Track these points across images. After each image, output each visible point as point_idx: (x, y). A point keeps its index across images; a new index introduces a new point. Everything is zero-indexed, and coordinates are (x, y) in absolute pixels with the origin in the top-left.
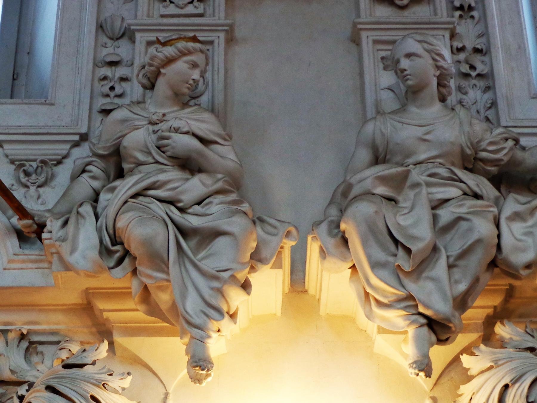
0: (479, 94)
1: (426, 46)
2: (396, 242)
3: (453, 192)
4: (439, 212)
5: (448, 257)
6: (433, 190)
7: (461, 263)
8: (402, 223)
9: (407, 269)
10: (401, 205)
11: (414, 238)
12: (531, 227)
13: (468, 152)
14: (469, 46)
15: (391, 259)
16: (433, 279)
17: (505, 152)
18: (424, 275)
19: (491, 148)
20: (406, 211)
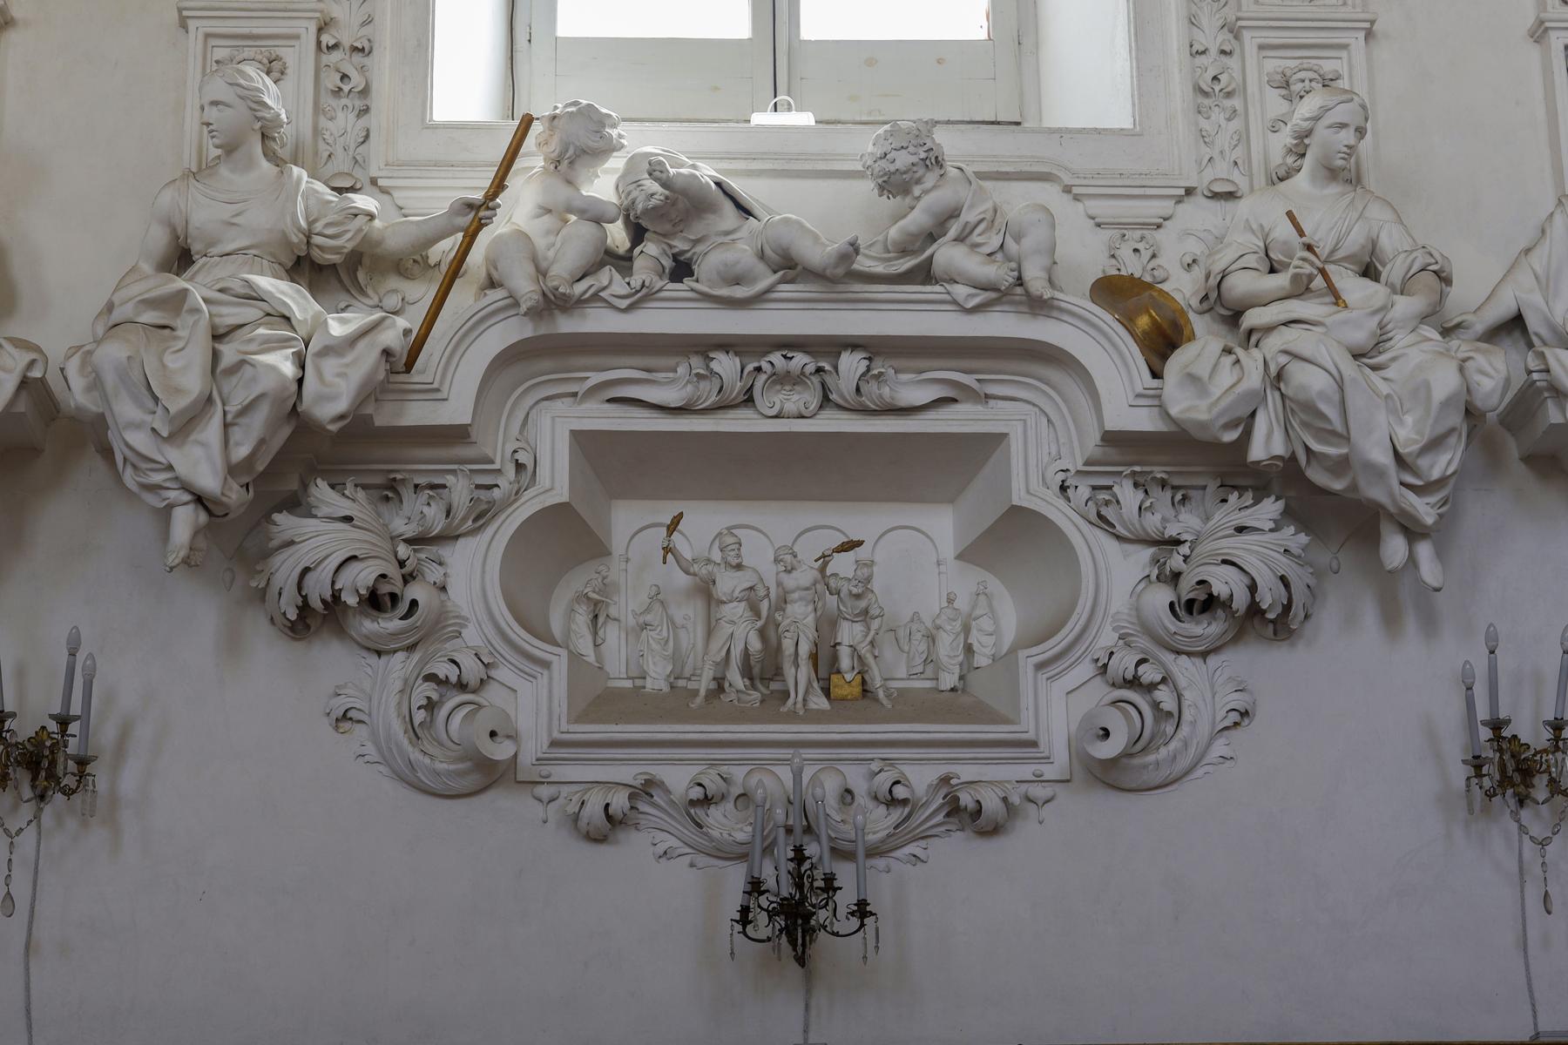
0: (352, 117)
1: (239, 90)
2: (156, 399)
3: (250, 313)
4: (222, 347)
5: (225, 413)
6: (224, 310)
7: (241, 420)
8: (170, 365)
9: (165, 434)
10: (179, 333)
11: (178, 391)
12: (347, 365)
13: (295, 240)
14: (346, 42)
15: (149, 418)
16: (202, 444)
17: (349, 235)
18: (192, 437)
19: (329, 231)
20: (181, 344)
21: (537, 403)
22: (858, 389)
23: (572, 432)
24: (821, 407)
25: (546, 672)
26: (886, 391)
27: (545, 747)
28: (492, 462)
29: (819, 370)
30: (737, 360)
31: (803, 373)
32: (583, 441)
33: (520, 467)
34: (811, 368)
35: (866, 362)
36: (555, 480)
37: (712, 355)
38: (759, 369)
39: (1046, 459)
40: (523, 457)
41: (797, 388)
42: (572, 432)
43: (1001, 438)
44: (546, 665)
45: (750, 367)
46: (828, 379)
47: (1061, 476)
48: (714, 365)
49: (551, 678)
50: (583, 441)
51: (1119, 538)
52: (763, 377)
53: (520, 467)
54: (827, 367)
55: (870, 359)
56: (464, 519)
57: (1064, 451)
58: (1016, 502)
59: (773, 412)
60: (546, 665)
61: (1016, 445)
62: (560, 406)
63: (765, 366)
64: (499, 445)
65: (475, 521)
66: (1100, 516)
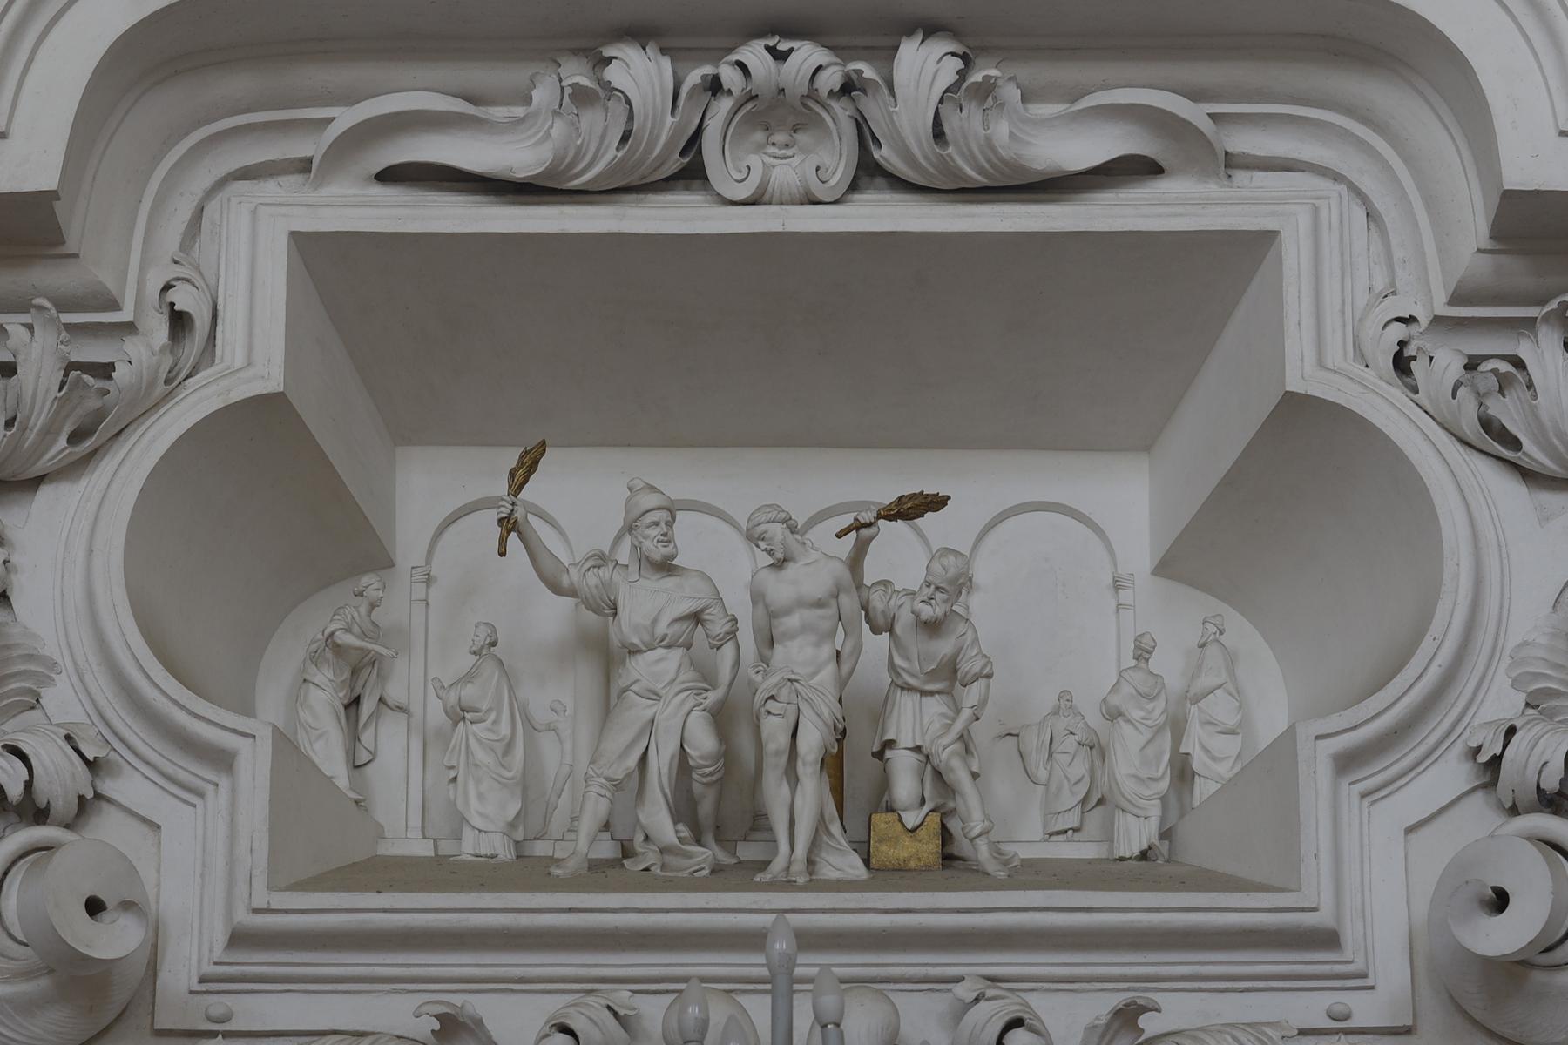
21: (221, 183)
22: (938, 134)
23: (295, 236)
24: (854, 187)
25: (224, 782)
26: (1001, 130)
27: (218, 953)
28: (115, 306)
29: (848, 88)
30: (666, 63)
31: (812, 94)
32: (315, 253)
33: (179, 321)
34: (831, 79)
35: (958, 64)
36: (255, 345)
37: (608, 52)
38: (714, 86)
39: (1362, 299)
40: (182, 298)
41: (802, 138)
42: (295, 236)
43: (1268, 238)
44: (222, 760)
45: (694, 77)
46: (873, 108)
47: (1399, 331)
48: (613, 74)
49: (233, 790)
50: (315, 253)
51: (1528, 475)
52: (724, 105)
53: (179, 321)
54: (869, 72)
55: (965, 58)
56: (49, 432)
57: (1403, 277)
58: (1294, 385)
59: (744, 192)
60: (222, 760)
61: (1294, 255)
62: (270, 189)
63: (730, 76)
64: (126, 258)
65: (75, 438)
66: (1487, 424)
